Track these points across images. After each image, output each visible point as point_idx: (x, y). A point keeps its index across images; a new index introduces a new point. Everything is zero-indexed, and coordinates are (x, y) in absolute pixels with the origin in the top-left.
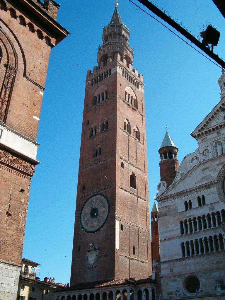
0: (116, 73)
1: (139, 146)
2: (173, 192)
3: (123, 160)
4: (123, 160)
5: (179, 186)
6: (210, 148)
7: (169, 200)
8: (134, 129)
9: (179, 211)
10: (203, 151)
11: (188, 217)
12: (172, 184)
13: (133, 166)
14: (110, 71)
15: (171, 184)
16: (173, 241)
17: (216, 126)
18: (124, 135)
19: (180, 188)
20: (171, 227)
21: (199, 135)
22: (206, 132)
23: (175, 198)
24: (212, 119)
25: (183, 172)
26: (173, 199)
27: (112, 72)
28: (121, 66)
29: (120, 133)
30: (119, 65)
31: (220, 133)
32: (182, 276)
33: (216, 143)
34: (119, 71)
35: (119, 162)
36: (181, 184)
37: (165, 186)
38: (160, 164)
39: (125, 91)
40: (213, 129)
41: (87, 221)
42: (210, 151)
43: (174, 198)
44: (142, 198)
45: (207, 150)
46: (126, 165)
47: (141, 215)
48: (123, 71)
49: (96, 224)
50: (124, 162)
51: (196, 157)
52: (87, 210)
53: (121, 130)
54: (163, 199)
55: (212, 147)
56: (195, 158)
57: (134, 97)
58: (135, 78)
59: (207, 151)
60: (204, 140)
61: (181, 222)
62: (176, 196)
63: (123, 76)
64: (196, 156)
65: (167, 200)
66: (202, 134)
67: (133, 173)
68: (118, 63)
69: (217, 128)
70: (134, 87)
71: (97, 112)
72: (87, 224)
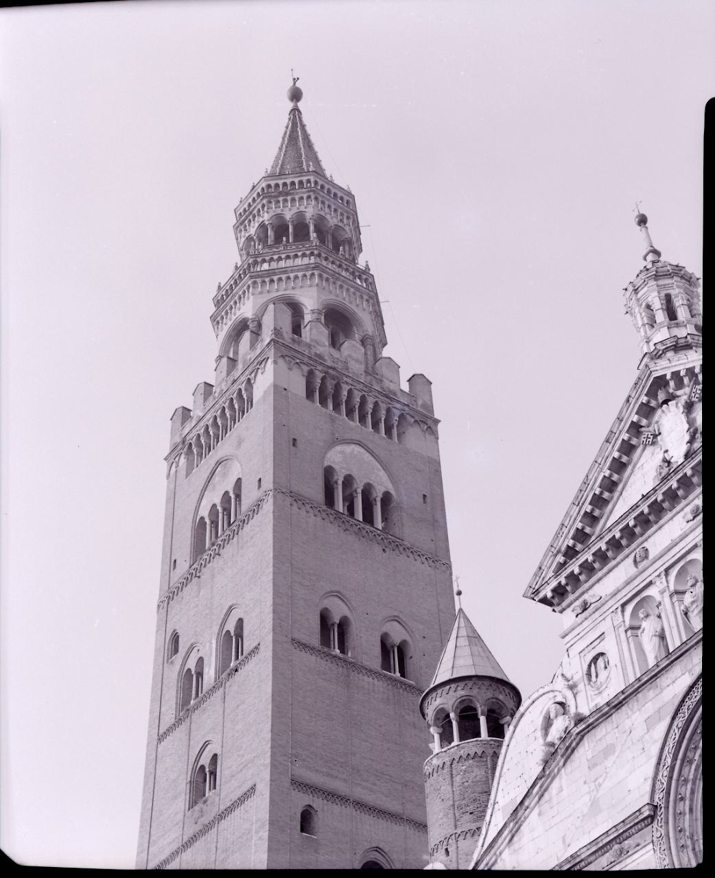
6: (609, 646)
10: (585, 667)
17: (621, 526)
21: (560, 592)
22: (588, 568)
24: (606, 495)
25: (512, 795)
31: (646, 557)
33: (634, 613)
39: (326, 464)
40: (615, 545)
42: (613, 656)
45: (602, 654)
48: (310, 377)
51: (562, 704)
53: (304, 646)
55: (623, 635)
57: (382, 483)
59: (600, 662)
60: (585, 607)
64: (560, 699)
66: (574, 579)
67: (378, 849)
69: (629, 533)
70: (379, 439)
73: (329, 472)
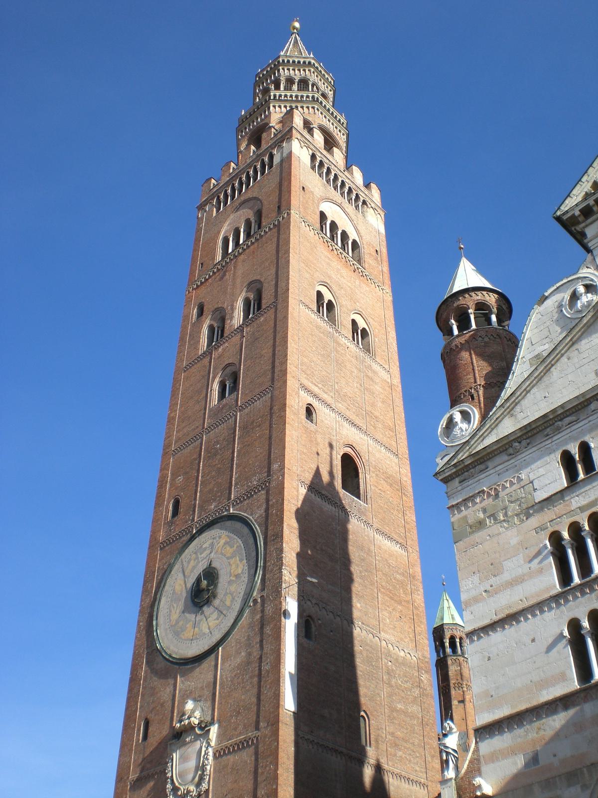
0: (288, 160)
1: (374, 372)
2: (508, 427)
3: (315, 396)
4: (315, 396)
5: (525, 403)
7: (490, 464)
8: (354, 322)
9: (540, 496)
11: (582, 509)
12: (498, 404)
13: (353, 424)
14: (271, 157)
15: (494, 405)
16: (526, 627)
18: (318, 327)
19: (533, 409)
20: (514, 566)
23: (517, 452)
26: (506, 458)
27: (277, 160)
28: (307, 144)
29: (301, 315)
30: (299, 137)
32: (587, 775)
34: (300, 152)
35: (296, 401)
36: (536, 393)
37: (469, 422)
38: (442, 356)
41: (177, 622)
43: (511, 451)
44: (391, 539)
46: (321, 411)
47: (391, 598)
48: (313, 157)
49: (210, 625)
50: (316, 404)
52: (179, 584)
54: (467, 468)
56: (581, 289)
57: (353, 235)
58: (353, 186)
61: (555, 538)
62: (519, 440)
63: (313, 168)
65: (482, 467)
67: (351, 446)
68: (294, 131)
70: (350, 209)
71: (227, 277)
72: (177, 634)
73: (323, 216)
